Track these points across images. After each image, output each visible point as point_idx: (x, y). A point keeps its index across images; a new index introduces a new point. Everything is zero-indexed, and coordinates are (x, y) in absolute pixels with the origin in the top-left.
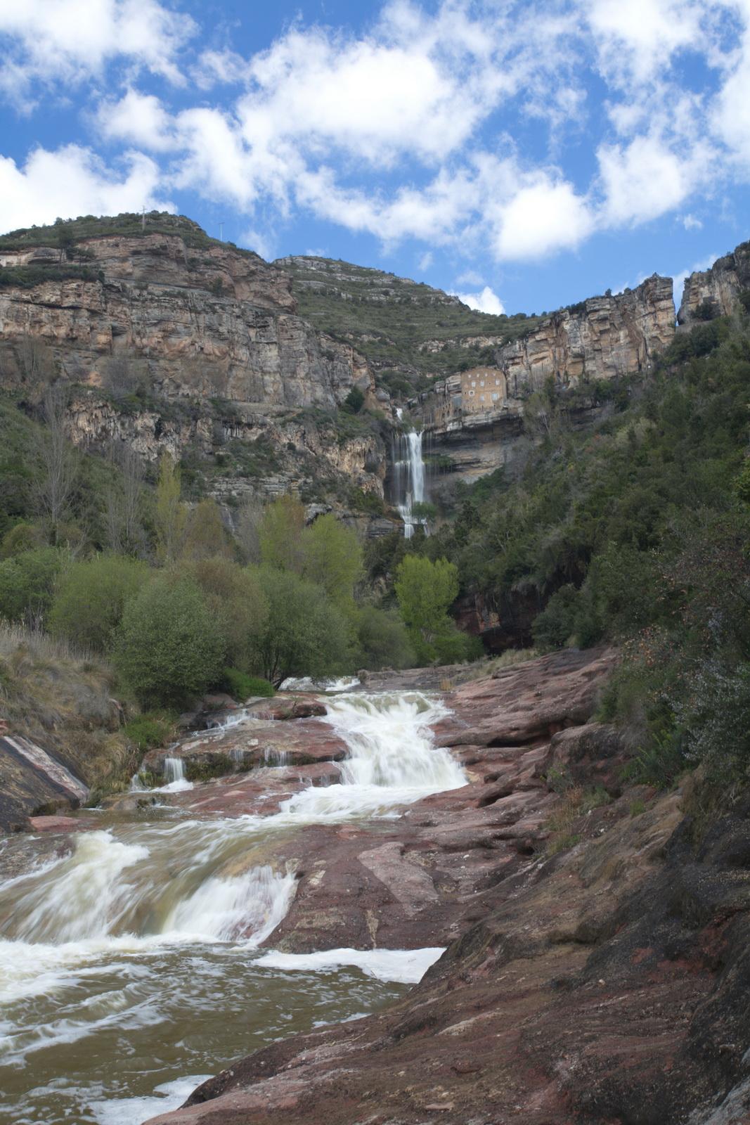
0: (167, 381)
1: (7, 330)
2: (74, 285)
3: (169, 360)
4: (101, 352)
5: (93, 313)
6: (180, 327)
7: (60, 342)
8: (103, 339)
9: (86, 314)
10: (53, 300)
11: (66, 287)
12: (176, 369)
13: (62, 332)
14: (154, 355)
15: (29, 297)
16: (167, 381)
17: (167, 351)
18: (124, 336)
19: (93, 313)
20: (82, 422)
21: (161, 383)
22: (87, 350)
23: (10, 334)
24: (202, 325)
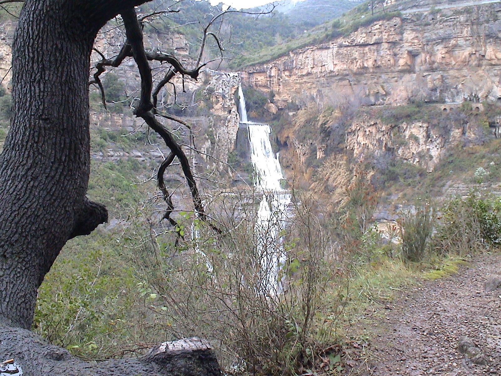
0: (460, 86)
1: (337, 68)
2: (378, 26)
3: (457, 69)
4: (403, 72)
5: (394, 44)
6: (461, 42)
7: (371, 70)
8: (402, 62)
9: (385, 46)
10: (362, 41)
11: (373, 28)
12: (465, 76)
13: (369, 63)
14: (444, 67)
15: (347, 44)
16: (460, 86)
17: (453, 63)
18: (420, 56)
19: (394, 44)
20: (360, 139)
21: (456, 88)
22: (392, 72)
23: (338, 71)
24: (482, 35)
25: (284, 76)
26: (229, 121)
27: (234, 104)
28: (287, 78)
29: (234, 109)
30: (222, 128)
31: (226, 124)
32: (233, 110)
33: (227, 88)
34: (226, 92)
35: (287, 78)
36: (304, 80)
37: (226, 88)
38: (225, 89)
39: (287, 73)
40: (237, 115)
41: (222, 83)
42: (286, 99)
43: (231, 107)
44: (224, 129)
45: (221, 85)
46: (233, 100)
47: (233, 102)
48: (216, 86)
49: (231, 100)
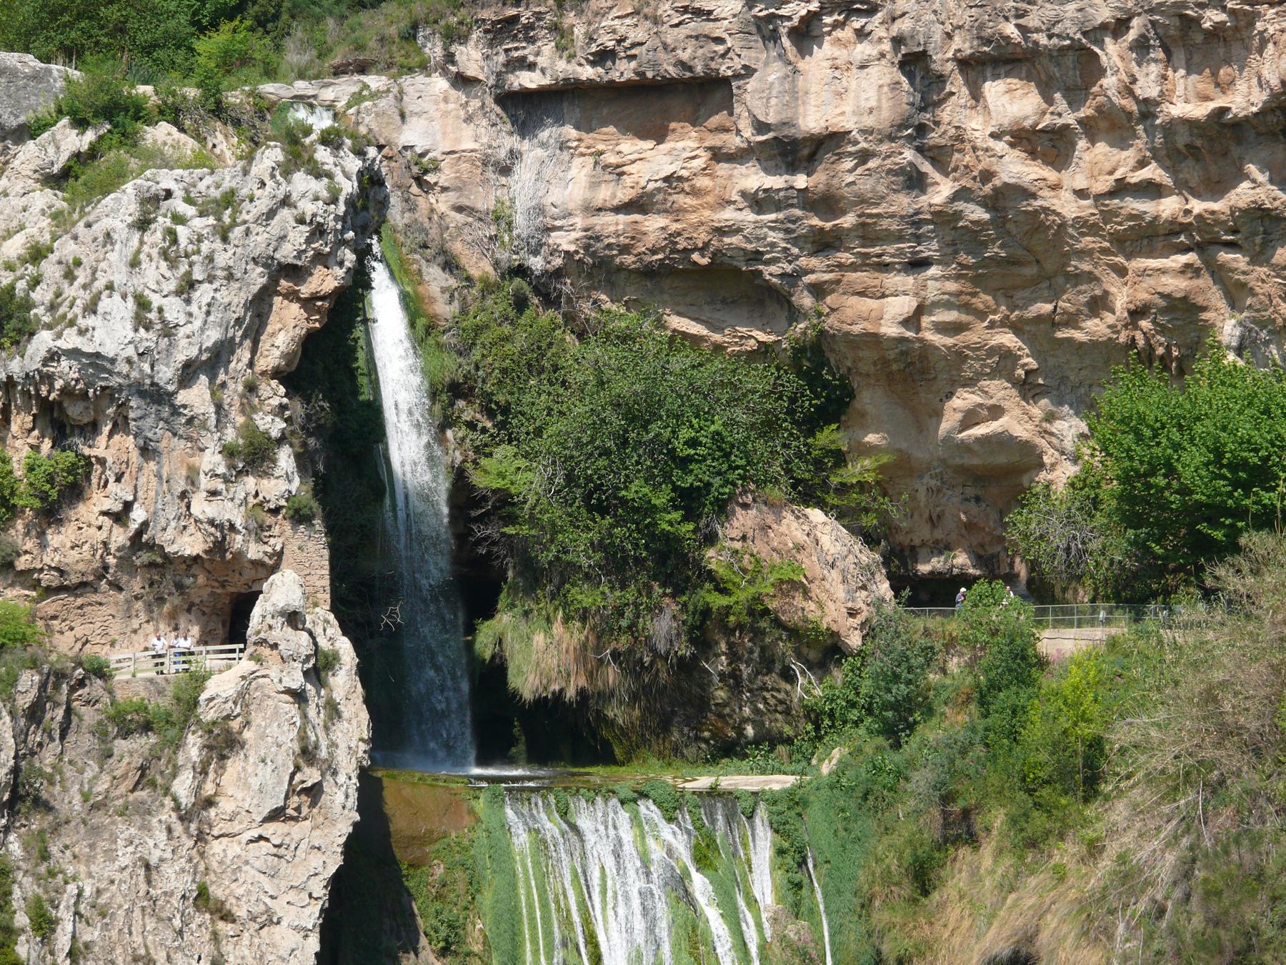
25: (977, 127)
26: (224, 743)
27: (299, 517)
28: (1016, 168)
29: (297, 581)
30: (125, 831)
31: (183, 786)
32: (282, 590)
33: (203, 294)
34: (185, 351)
35: (1016, 168)
36: (1242, 195)
37: (187, 287)
38: (174, 310)
39: (1012, 101)
40: (320, 668)
41: (143, 224)
42: (1003, 441)
43: (254, 551)
44: (156, 845)
45: (116, 259)
46: (285, 459)
47: (284, 479)
48: (50, 269)
49: (253, 456)
